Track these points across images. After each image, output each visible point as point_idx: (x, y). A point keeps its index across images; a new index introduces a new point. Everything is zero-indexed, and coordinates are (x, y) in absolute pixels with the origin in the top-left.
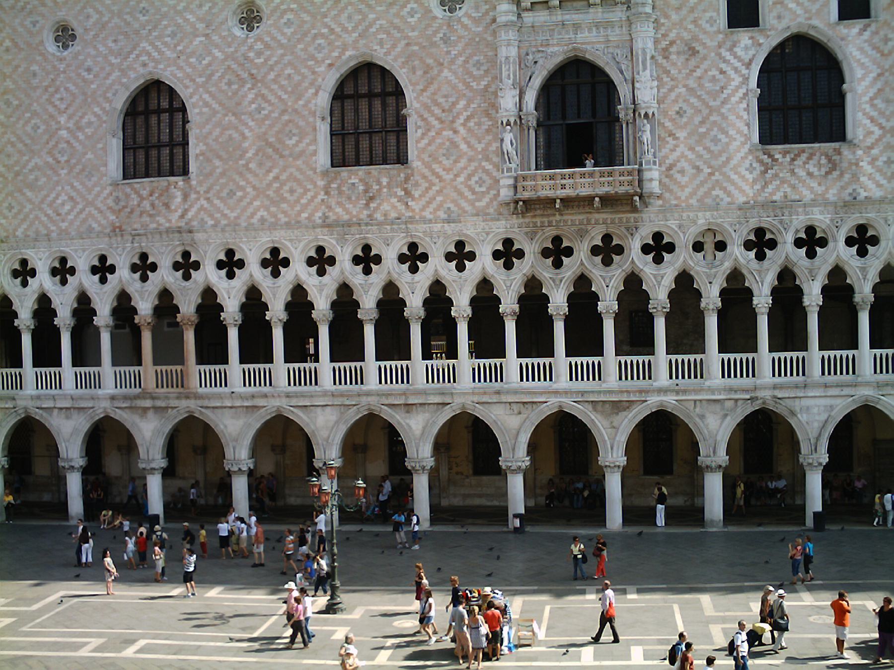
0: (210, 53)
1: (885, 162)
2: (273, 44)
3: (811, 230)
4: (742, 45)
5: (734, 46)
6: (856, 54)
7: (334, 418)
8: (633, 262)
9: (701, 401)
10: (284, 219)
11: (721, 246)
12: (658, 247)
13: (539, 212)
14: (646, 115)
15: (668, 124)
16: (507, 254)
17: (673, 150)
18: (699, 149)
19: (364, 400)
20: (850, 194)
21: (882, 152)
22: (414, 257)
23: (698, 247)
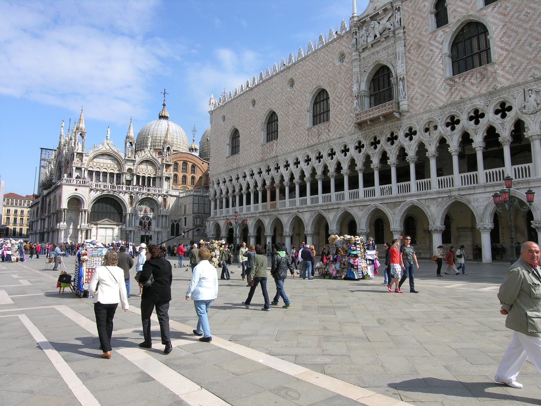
0: (282, 98)
1: (510, 67)
2: (296, 90)
3: (476, 111)
4: (439, 36)
5: (436, 37)
6: (491, 20)
7: (309, 216)
8: (400, 142)
9: (427, 199)
10: (298, 148)
11: (436, 127)
12: (411, 134)
13: (366, 128)
14: (400, 78)
15: (411, 80)
16: (359, 147)
17: (413, 90)
18: (423, 87)
19: (317, 208)
20: (493, 88)
21: (508, 63)
22: (332, 154)
23: (427, 130)
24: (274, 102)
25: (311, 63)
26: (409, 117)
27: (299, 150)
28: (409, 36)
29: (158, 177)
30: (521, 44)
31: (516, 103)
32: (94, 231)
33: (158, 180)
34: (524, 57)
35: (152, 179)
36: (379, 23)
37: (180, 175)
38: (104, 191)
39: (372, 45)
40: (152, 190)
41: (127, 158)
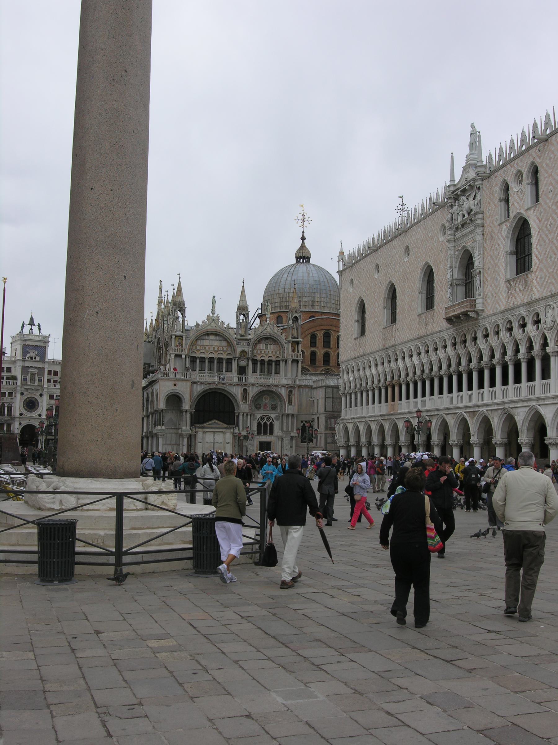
16: (454, 344)
18: (493, 285)
24: (393, 273)
25: (422, 232)
26: (483, 318)
27: (412, 340)
28: (486, 222)
29: (282, 360)
30: (546, 256)
31: (542, 316)
32: (200, 435)
33: (282, 364)
34: (547, 270)
35: (273, 364)
36: (468, 199)
37: (320, 352)
38: (209, 384)
39: (463, 226)
40: (272, 380)
41: (239, 337)
